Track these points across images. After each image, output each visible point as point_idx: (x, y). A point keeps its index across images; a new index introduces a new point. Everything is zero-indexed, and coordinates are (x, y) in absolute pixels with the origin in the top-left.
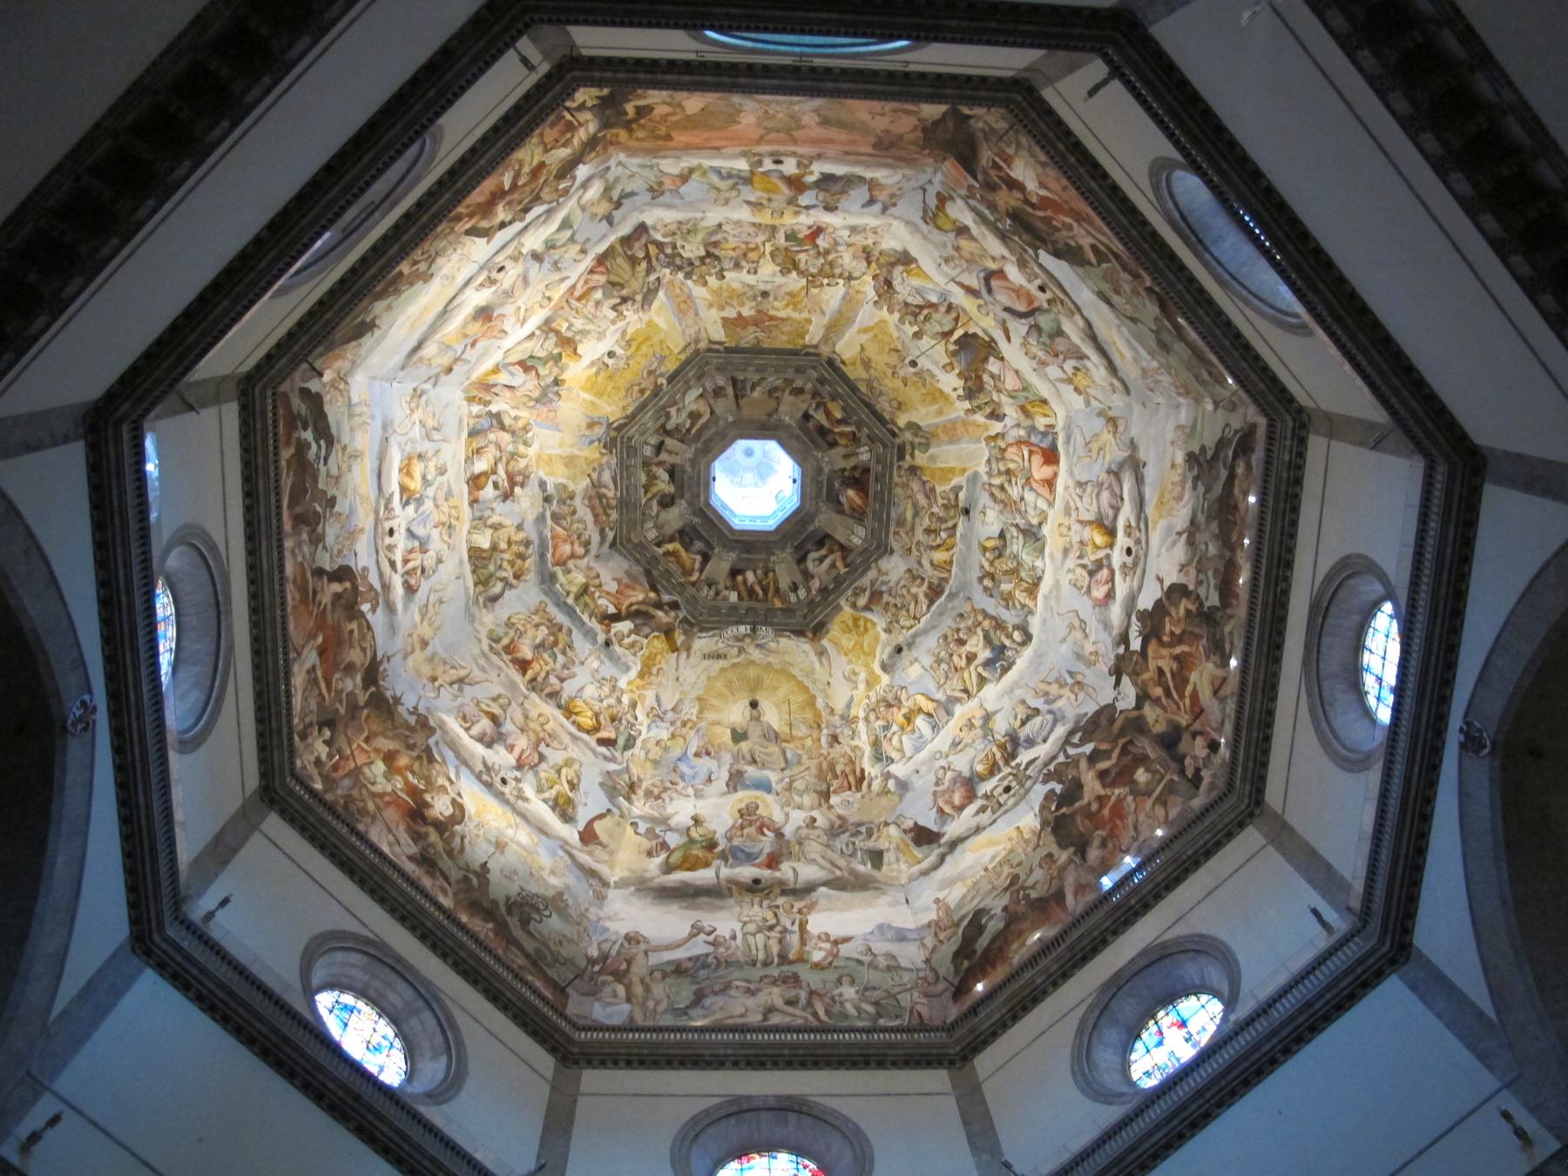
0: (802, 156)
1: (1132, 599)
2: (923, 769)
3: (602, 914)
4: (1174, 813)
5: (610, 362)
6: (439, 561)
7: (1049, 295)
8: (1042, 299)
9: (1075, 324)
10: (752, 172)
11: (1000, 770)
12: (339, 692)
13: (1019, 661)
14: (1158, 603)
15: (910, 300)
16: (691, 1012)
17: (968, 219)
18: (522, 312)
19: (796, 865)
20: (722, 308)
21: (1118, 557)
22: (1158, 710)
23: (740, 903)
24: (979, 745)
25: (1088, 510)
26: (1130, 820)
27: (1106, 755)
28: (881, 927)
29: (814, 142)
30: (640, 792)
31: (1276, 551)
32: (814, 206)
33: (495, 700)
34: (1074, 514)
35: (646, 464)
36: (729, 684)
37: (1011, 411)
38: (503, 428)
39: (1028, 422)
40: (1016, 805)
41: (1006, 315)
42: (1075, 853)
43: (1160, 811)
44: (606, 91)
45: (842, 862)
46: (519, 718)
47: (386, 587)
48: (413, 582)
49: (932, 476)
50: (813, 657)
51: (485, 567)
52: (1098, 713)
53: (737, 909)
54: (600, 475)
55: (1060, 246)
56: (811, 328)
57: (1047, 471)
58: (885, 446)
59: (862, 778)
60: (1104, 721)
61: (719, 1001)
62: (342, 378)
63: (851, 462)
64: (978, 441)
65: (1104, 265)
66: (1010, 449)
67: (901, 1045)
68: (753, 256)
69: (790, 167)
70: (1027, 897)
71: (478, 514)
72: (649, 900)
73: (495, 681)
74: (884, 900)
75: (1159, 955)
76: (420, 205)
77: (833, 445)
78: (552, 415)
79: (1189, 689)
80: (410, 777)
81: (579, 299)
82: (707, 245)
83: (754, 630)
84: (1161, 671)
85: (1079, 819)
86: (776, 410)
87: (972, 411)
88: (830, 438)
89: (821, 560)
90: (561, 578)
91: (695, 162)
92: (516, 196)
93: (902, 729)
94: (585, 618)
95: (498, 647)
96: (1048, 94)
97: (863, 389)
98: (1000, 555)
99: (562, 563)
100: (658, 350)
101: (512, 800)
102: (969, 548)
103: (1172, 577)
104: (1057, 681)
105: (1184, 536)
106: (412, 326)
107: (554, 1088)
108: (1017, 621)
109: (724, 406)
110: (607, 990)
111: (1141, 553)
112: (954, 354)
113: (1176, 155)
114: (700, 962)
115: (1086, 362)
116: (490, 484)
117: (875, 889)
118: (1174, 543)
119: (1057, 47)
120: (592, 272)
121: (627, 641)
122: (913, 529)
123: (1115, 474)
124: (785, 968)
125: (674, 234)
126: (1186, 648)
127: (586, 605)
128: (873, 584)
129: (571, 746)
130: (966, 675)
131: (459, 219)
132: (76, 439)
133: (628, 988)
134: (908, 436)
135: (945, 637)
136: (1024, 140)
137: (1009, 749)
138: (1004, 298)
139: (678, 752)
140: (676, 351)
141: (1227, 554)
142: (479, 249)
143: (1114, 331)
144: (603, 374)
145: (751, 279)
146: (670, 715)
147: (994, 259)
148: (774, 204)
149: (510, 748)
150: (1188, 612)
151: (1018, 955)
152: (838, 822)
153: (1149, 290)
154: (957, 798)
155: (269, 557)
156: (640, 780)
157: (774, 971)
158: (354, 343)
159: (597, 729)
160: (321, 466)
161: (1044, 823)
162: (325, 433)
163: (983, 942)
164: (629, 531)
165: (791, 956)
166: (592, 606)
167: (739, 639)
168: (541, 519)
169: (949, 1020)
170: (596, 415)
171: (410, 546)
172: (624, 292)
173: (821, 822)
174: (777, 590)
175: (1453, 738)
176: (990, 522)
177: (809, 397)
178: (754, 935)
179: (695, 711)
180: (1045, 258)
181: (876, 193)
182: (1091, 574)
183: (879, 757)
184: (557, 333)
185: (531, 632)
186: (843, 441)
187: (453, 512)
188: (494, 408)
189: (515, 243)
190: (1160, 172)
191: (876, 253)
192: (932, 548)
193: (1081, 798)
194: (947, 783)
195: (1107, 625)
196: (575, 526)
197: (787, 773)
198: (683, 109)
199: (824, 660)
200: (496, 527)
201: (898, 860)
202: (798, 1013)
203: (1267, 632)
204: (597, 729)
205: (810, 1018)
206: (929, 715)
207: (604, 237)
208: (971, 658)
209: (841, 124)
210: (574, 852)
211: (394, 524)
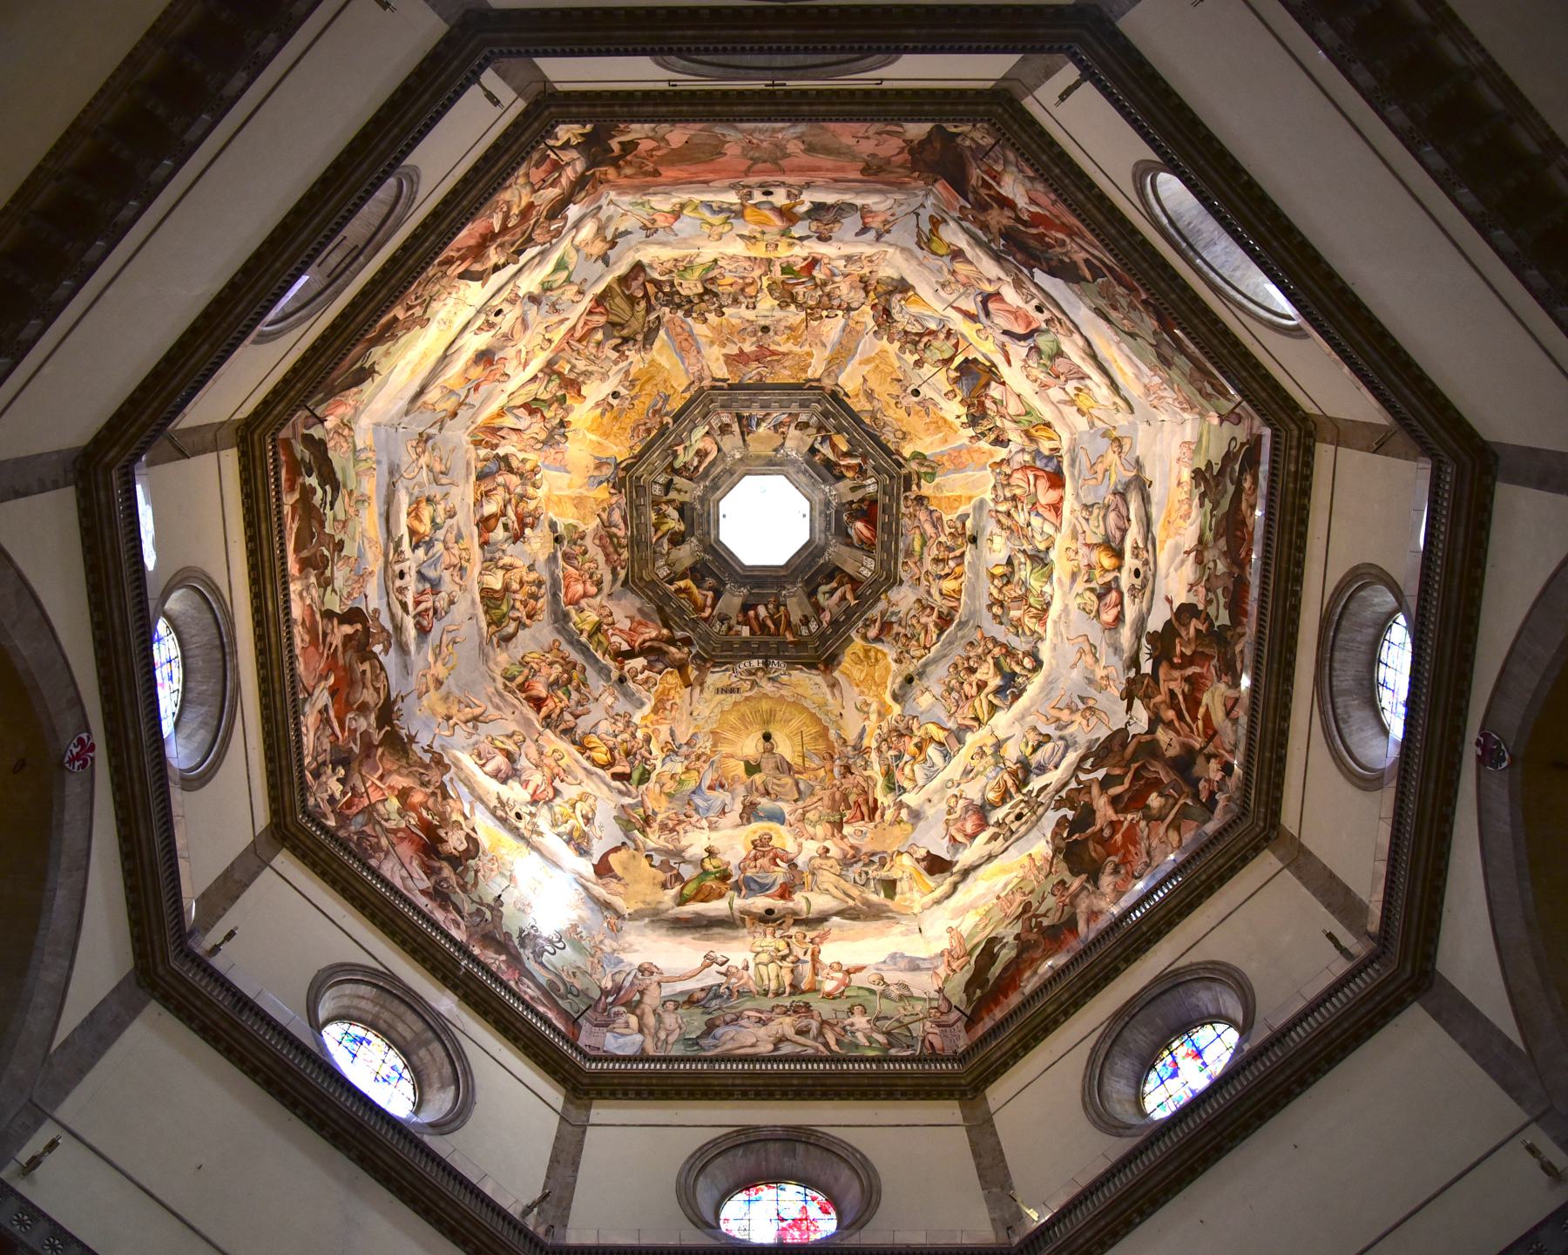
0: (790, 186)
1: (1141, 621)
2: (935, 799)
3: (615, 945)
4: (1188, 837)
5: (615, 402)
6: (452, 602)
7: (1046, 315)
8: (1039, 319)
9: (1077, 344)
10: (742, 204)
11: (1011, 798)
12: (353, 732)
13: (1028, 688)
14: (1168, 624)
15: (909, 328)
16: (702, 1042)
17: (962, 242)
18: (523, 355)
19: (809, 895)
20: (724, 345)
21: (1126, 580)
22: (1172, 734)
23: (752, 933)
24: (990, 772)
25: (1095, 534)
26: (1143, 846)
27: (1118, 780)
28: (893, 956)
29: (801, 170)
30: (655, 826)
31: (1284, 565)
32: (808, 237)
33: (509, 736)
34: (1081, 537)
35: (656, 503)
36: (742, 718)
37: (1016, 438)
38: (511, 470)
39: (1034, 447)
40: (1028, 831)
41: (1005, 339)
42: (1087, 881)
43: (1173, 836)
44: (589, 127)
45: (855, 892)
46: (534, 754)
47: (398, 628)
48: (425, 623)
49: (939, 506)
50: (827, 690)
51: (498, 607)
52: (1110, 738)
53: (750, 939)
54: (610, 514)
55: (1054, 263)
56: (813, 361)
57: (1052, 496)
58: (891, 477)
59: (875, 808)
60: (1116, 748)
61: (731, 1031)
62: (346, 424)
63: (859, 494)
64: (984, 468)
65: (1100, 280)
66: (1016, 475)
67: (911, 1075)
68: (750, 291)
69: (780, 198)
70: (1039, 924)
71: (488, 556)
72: (663, 931)
73: (507, 722)
74: (897, 929)
75: (1172, 982)
76: (405, 248)
77: (841, 477)
78: (559, 456)
79: (1202, 710)
80: (424, 813)
81: (580, 341)
82: (704, 281)
83: (766, 664)
84: (1172, 693)
85: (1091, 845)
86: (783, 444)
87: (977, 438)
88: (836, 472)
89: (832, 592)
90: (574, 616)
91: (685, 197)
92: (507, 238)
93: (914, 757)
94: (599, 655)
95: (513, 685)
96: (1029, 103)
97: (867, 421)
98: (1008, 582)
99: (575, 603)
100: (662, 390)
101: (527, 834)
102: (977, 575)
103: (1181, 597)
104: (1068, 707)
105: (1193, 554)
106: (413, 372)
107: (562, 1118)
108: (1027, 647)
109: (732, 443)
110: (621, 1020)
111: (1150, 574)
112: (956, 381)
113: (1154, 157)
114: (712, 992)
115: (1088, 382)
116: (500, 525)
117: (888, 918)
118: (1183, 562)
119: (1033, 50)
120: (590, 313)
121: (640, 677)
122: (921, 559)
123: (1122, 495)
124: (796, 998)
125: (671, 271)
126: (1197, 670)
127: (600, 643)
128: (883, 614)
129: (586, 781)
130: (977, 703)
131: (449, 262)
132: (66, 485)
133: (640, 1018)
134: (914, 466)
135: (956, 666)
136: (1011, 156)
137: (1020, 776)
138: (1003, 321)
139: (691, 785)
140: (681, 390)
141: (1236, 571)
142: (475, 293)
143: (1114, 348)
144: (608, 414)
145: (750, 315)
146: (684, 749)
147: (990, 281)
148: (767, 237)
149: (525, 784)
150: (1198, 631)
151: (1029, 984)
152: (851, 852)
153: (1144, 302)
154: (969, 828)
155: (275, 600)
156: (655, 814)
157: (786, 1001)
158: (355, 390)
159: (611, 764)
160: (327, 511)
161: (1056, 851)
162: (329, 477)
163: (996, 970)
164: (640, 571)
165: (803, 986)
166: (606, 644)
167: (750, 673)
168: (552, 559)
169: (960, 1050)
170: (603, 455)
171: (421, 588)
172: (625, 332)
173: (835, 852)
174: (789, 623)
175: (1470, 753)
176: (997, 549)
177: (815, 431)
178: (767, 965)
179: (708, 744)
180: (1041, 277)
181: (867, 220)
182: (1100, 597)
183: (892, 786)
184: (560, 374)
185: (545, 670)
186: (850, 474)
187: (464, 554)
188: (501, 451)
189: (511, 286)
190: (1142, 172)
191: (873, 282)
192: (940, 577)
193: (1094, 824)
194: (959, 813)
195: (1117, 649)
196: (587, 566)
197: (800, 804)
198: (668, 143)
199: (836, 692)
200: (508, 568)
201: (911, 889)
202: (810, 1042)
203: (1277, 648)
204: (611, 764)
205: (821, 1048)
206: (941, 744)
207: (600, 277)
208: (981, 686)
209: (827, 151)
210: (589, 884)
211: (405, 566)
